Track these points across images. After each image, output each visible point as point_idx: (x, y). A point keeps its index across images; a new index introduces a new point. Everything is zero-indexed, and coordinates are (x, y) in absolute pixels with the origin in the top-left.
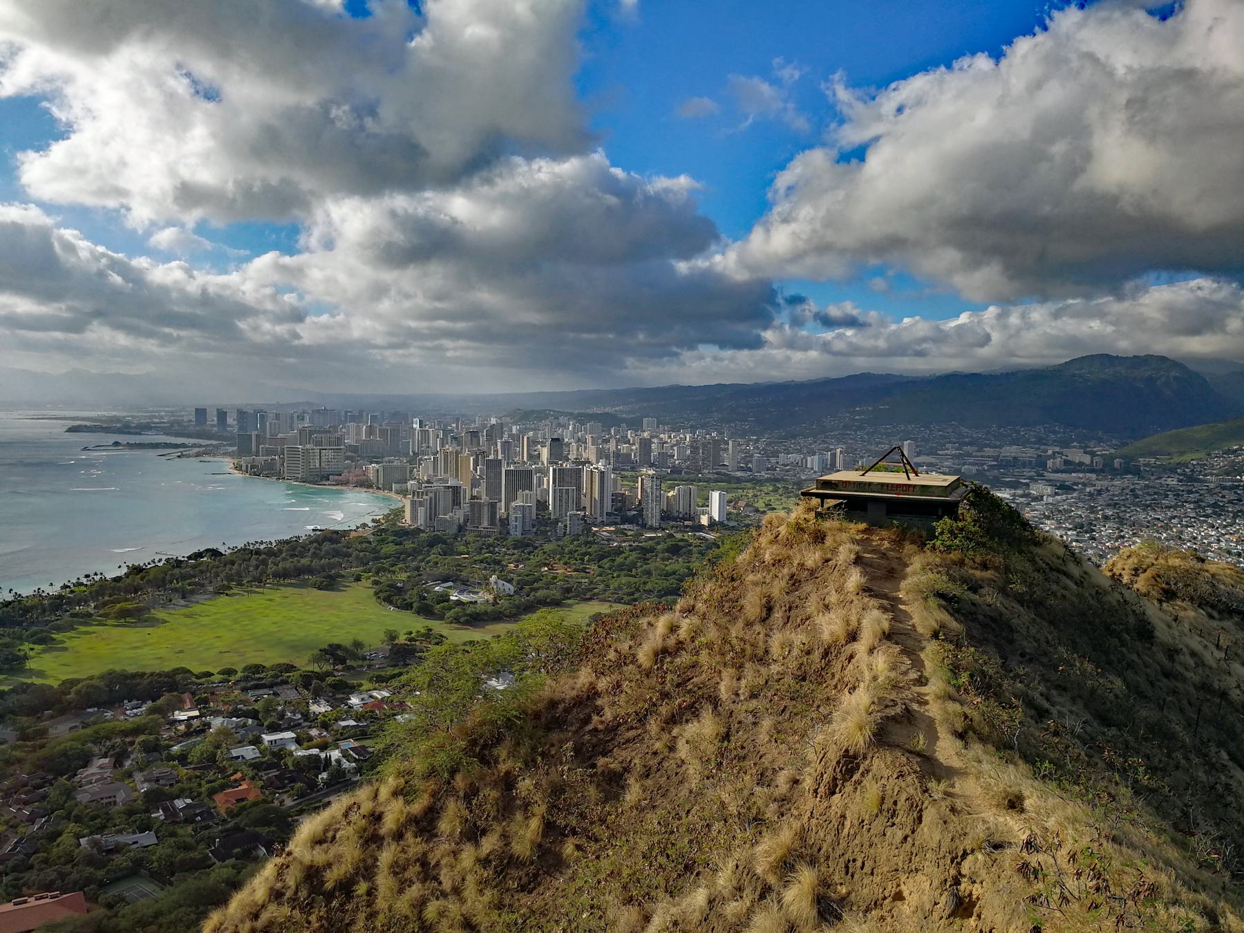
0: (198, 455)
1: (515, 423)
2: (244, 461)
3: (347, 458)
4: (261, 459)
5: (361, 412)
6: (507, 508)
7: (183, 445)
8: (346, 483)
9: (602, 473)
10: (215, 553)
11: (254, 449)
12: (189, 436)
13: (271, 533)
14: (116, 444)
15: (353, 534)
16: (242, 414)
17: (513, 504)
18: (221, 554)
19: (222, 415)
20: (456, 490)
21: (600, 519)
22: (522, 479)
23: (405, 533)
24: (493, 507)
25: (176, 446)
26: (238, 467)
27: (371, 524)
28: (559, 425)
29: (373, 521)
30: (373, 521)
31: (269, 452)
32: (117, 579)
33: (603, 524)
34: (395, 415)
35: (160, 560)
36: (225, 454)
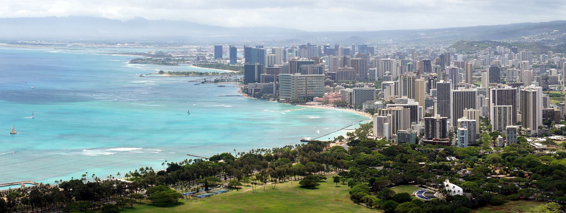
0: (216, 81)
1: (460, 52)
2: (251, 85)
3: (327, 83)
4: (261, 85)
5: (337, 47)
6: (455, 123)
7: (207, 74)
8: (326, 103)
9: (534, 93)
10: (228, 157)
11: (256, 77)
12: (210, 66)
13: (268, 143)
14: (161, 72)
15: (332, 145)
16: (248, 52)
17: (459, 120)
18: (233, 158)
19: (233, 51)
20: (414, 109)
21: (533, 132)
22: (467, 100)
23: (372, 144)
24: (443, 122)
25: (201, 74)
26: (246, 91)
27: (346, 137)
28: (496, 53)
29: (348, 134)
30: (348, 134)
31: (268, 80)
32: (161, 173)
33: (535, 136)
34: (363, 47)
35: (190, 161)
36: (236, 80)
